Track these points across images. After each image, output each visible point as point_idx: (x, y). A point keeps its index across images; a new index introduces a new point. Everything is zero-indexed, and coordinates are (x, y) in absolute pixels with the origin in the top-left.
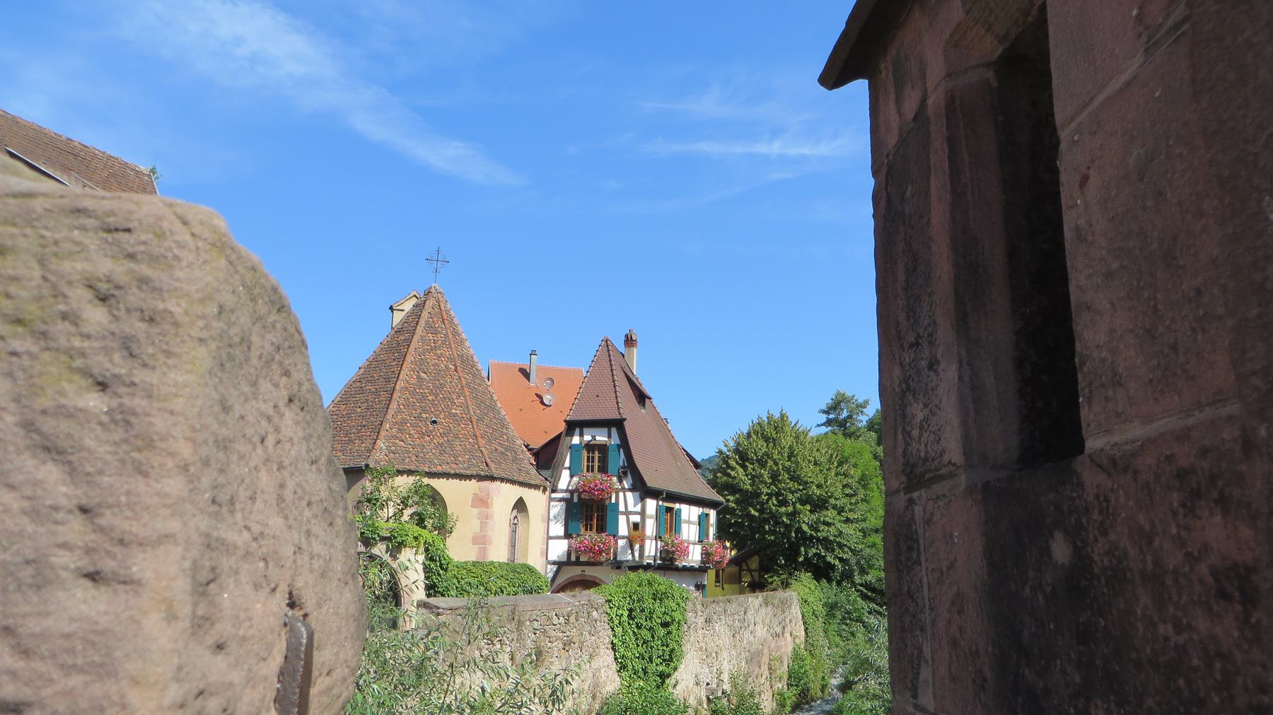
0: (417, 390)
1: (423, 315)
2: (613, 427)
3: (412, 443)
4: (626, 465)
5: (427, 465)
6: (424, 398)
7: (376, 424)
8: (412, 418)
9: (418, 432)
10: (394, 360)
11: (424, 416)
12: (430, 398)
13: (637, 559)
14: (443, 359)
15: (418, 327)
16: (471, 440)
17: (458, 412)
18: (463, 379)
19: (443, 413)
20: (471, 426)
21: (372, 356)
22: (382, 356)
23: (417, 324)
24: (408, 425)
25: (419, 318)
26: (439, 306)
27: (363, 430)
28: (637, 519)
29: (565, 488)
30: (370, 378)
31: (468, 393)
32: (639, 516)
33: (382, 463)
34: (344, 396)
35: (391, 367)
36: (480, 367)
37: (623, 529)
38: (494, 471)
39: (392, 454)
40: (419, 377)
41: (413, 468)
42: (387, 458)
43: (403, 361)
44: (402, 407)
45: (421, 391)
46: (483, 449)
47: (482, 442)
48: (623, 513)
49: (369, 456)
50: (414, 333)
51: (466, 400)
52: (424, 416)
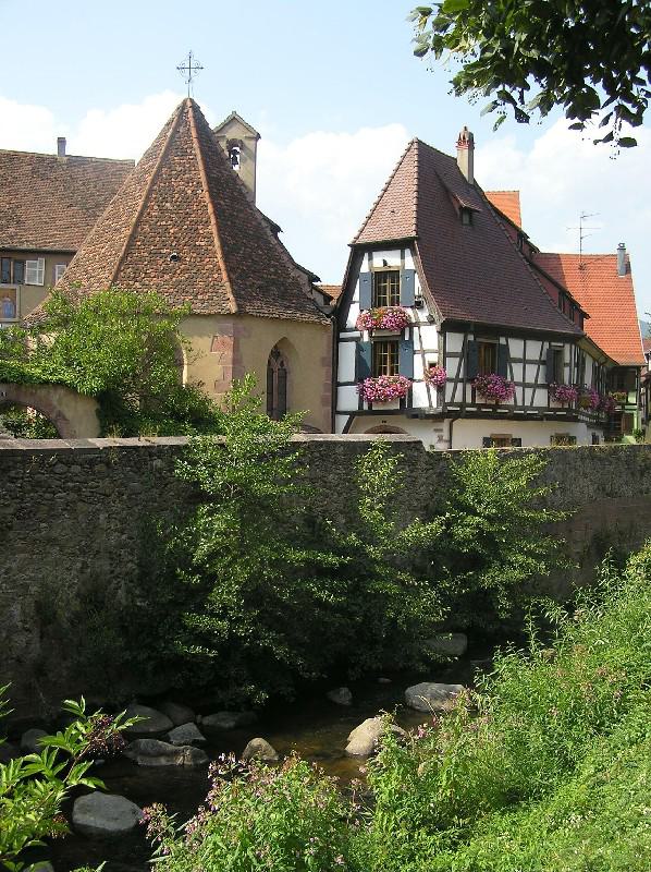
16: (216, 276)
17: (203, 244)
28: (433, 358)
37: (419, 373)
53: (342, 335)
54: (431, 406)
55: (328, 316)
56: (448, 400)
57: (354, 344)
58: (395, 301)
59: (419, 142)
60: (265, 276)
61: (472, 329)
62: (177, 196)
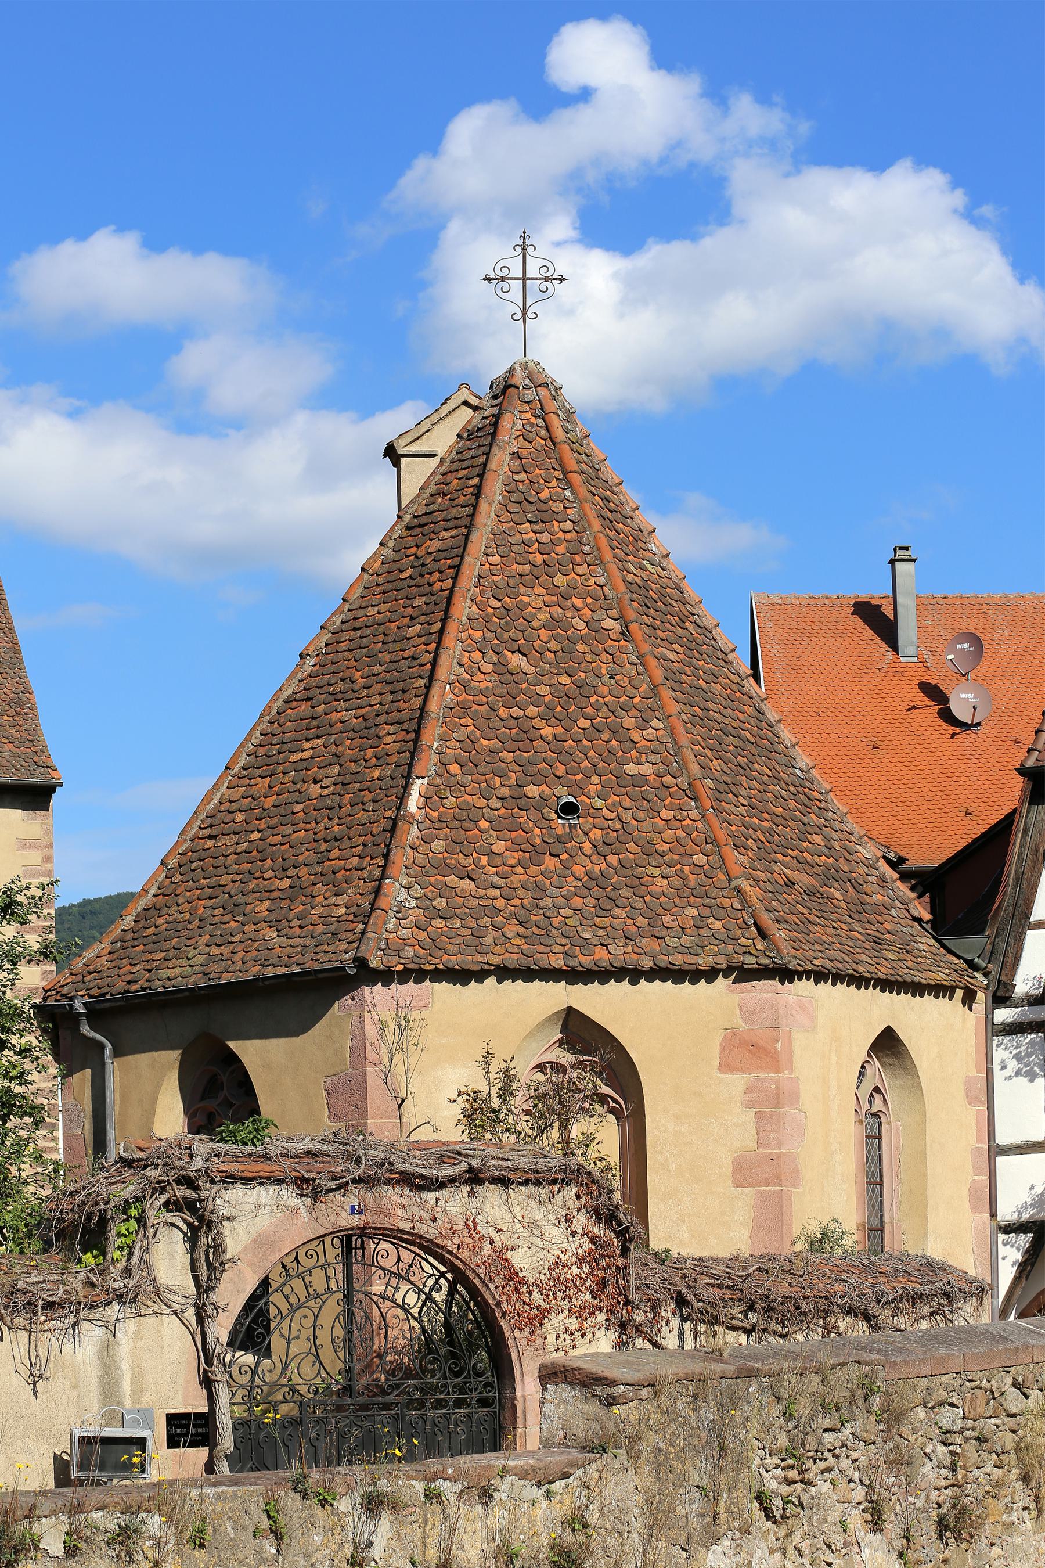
0: (503, 712)
1: (493, 465)
3: (501, 882)
5: (557, 949)
6: (526, 733)
7: (376, 829)
8: (495, 803)
9: (516, 846)
10: (412, 618)
11: (532, 791)
12: (548, 732)
14: (579, 603)
15: (483, 506)
16: (700, 859)
17: (647, 769)
18: (653, 663)
19: (595, 779)
20: (694, 814)
21: (338, 611)
22: (372, 611)
23: (477, 495)
24: (484, 824)
25: (481, 476)
26: (547, 428)
27: (336, 853)
30: (341, 686)
31: (673, 708)
33: (409, 952)
34: (261, 751)
35: (405, 644)
36: (708, 615)
38: (786, 949)
39: (438, 923)
40: (502, 669)
41: (512, 960)
42: (423, 935)
43: (444, 621)
44: (454, 768)
45: (516, 712)
46: (744, 885)
47: (733, 856)
49: (363, 933)
50: (470, 527)
51: (672, 730)
52: (532, 791)
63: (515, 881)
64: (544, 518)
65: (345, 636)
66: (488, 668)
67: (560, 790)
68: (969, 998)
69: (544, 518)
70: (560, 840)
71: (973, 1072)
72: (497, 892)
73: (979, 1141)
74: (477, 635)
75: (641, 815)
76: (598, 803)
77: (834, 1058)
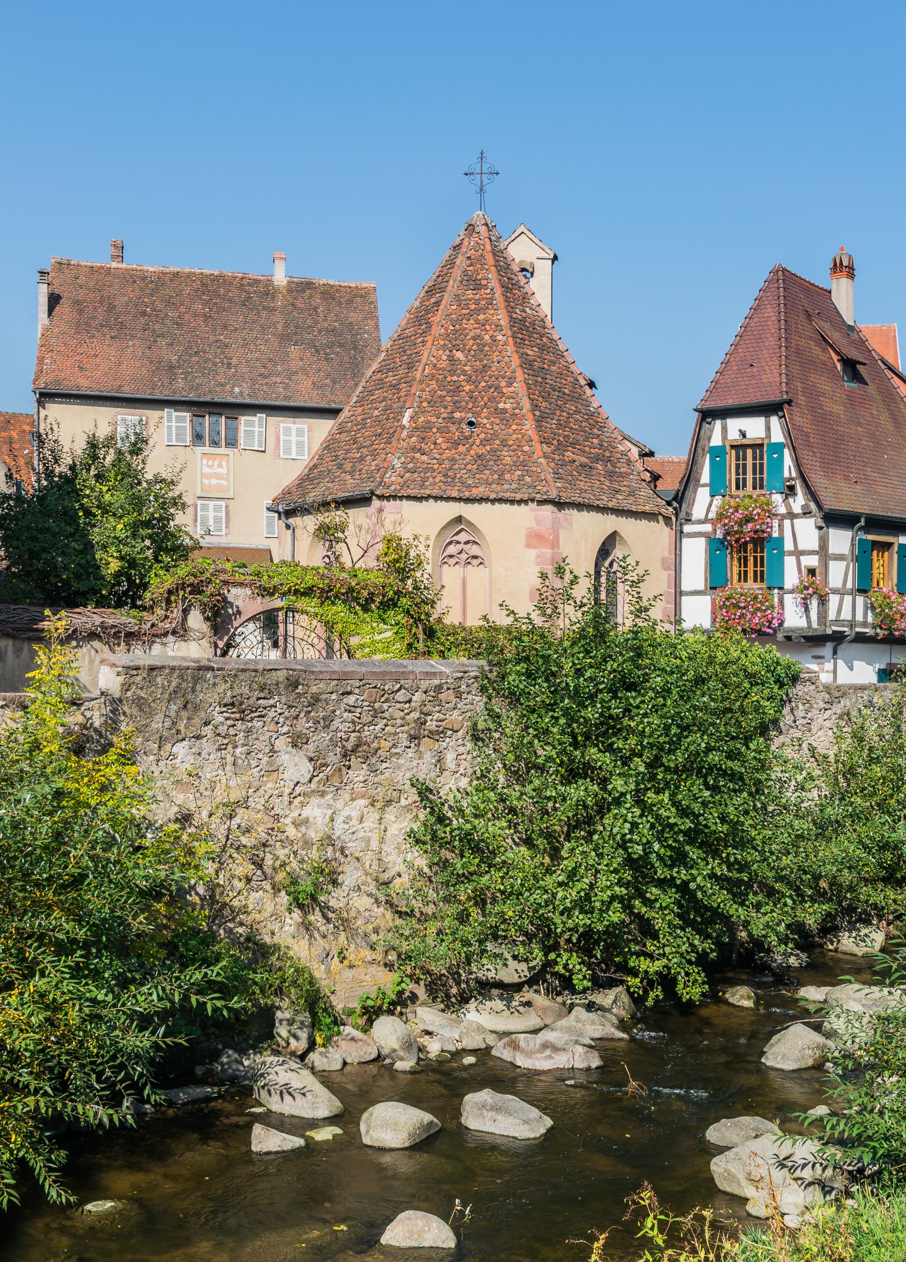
2: (773, 415)
4: (794, 475)
6: (458, 389)
8: (440, 420)
13: (815, 625)
17: (508, 406)
22: (408, 331)
24: (434, 430)
28: (812, 561)
29: (702, 517)
32: (816, 557)
37: (791, 577)
40: (451, 359)
44: (425, 404)
45: (455, 378)
48: (791, 553)
52: (457, 415)
53: (687, 528)
54: (810, 627)
55: (669, 503)
56: (832, 615)
57: (702, 541)
58: (759, 484)
59: (784, 270)
60: (587, 449)
61: (862, 523)
62: (471, 342)
63: (444, 457)
64: (478, 287)
65: (396, 343)
66: (445, 358)
67: (470, 415)
68: (667, 520)
69: (478, 287)
70: (467, 438)
71: (667, 555)
72: (436, 461)
73: (669, 587)
74: (442, 343)
75: (503, 427)
76: (485, 421)
77: (583, 544)
